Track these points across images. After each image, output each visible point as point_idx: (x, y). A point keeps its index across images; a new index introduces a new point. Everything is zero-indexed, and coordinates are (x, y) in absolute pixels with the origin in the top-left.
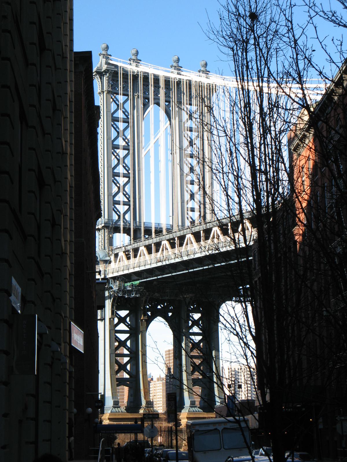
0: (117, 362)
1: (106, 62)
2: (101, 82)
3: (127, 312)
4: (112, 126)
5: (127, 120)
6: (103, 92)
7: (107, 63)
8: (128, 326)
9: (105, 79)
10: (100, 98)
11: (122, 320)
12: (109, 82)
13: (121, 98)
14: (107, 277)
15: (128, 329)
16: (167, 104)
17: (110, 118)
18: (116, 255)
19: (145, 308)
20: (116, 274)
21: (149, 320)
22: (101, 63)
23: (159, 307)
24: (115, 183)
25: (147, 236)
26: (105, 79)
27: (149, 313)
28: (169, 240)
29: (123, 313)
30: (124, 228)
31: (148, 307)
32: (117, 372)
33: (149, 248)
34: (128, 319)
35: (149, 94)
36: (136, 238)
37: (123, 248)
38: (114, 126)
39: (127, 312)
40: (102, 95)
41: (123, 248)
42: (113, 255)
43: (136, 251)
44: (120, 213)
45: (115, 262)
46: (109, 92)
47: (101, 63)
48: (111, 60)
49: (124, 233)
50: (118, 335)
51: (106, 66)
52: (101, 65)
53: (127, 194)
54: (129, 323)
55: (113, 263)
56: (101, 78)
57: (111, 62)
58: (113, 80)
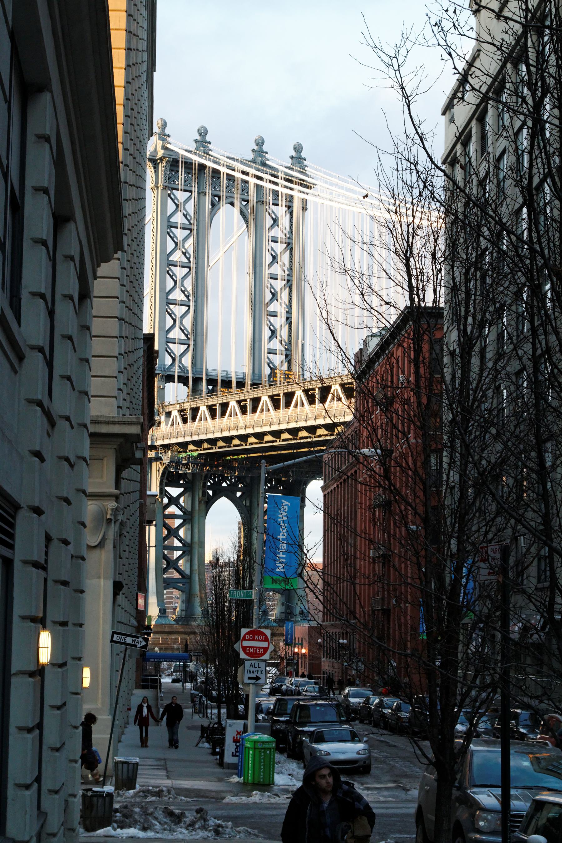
0: (165, 557)
1: (163, 146)
2: (155, 171)
3: (181, 490)
4: (168, 234)
5: (189, 227)
6: (157, 187)
7: (165, 148)
8: (181, 509)
9: (161, 168)
10: (153, 195)
11: (174, 501)
12: (165, 174)
13: (181, 196)
14: (156, 444)
15: (181, 513)
16: (244, 203)
17: (166, 224)
18: (169, 414)
19: (204, 485)
20: (167, 442)
21: (209, 502)
22: (156, 146)
23: (224, 484)
24: (169, 313)
25: (210, 387)
26: (161, 168)
27: (210, 492)
28: (239, 402)
29: (175, 492)
30: (180, 377)
31: (209, 484)
32: (165, 570)
33: (212, 409)
34: (181, 500)
35: (220, 190)
36: (195, 391)
37: (178, 406)
38: (171, 234)
39: (181, 490)
40: (155, 192)
41: (178, 406)
42: (164, 413)
43: (195, 410)
44: (175, 355)
45: (167, 425)
46: (165, 188)
47: (156, 146)
48: (170, 143)
49: (180, 382)
50: (167, 521)
51: (163, 151)
52: (156, 150)
53: (185, 329)
54: (183, 504)
55: (163, 425)
56: (154, 168)
57: (169, 146)
58: (171, 170)
